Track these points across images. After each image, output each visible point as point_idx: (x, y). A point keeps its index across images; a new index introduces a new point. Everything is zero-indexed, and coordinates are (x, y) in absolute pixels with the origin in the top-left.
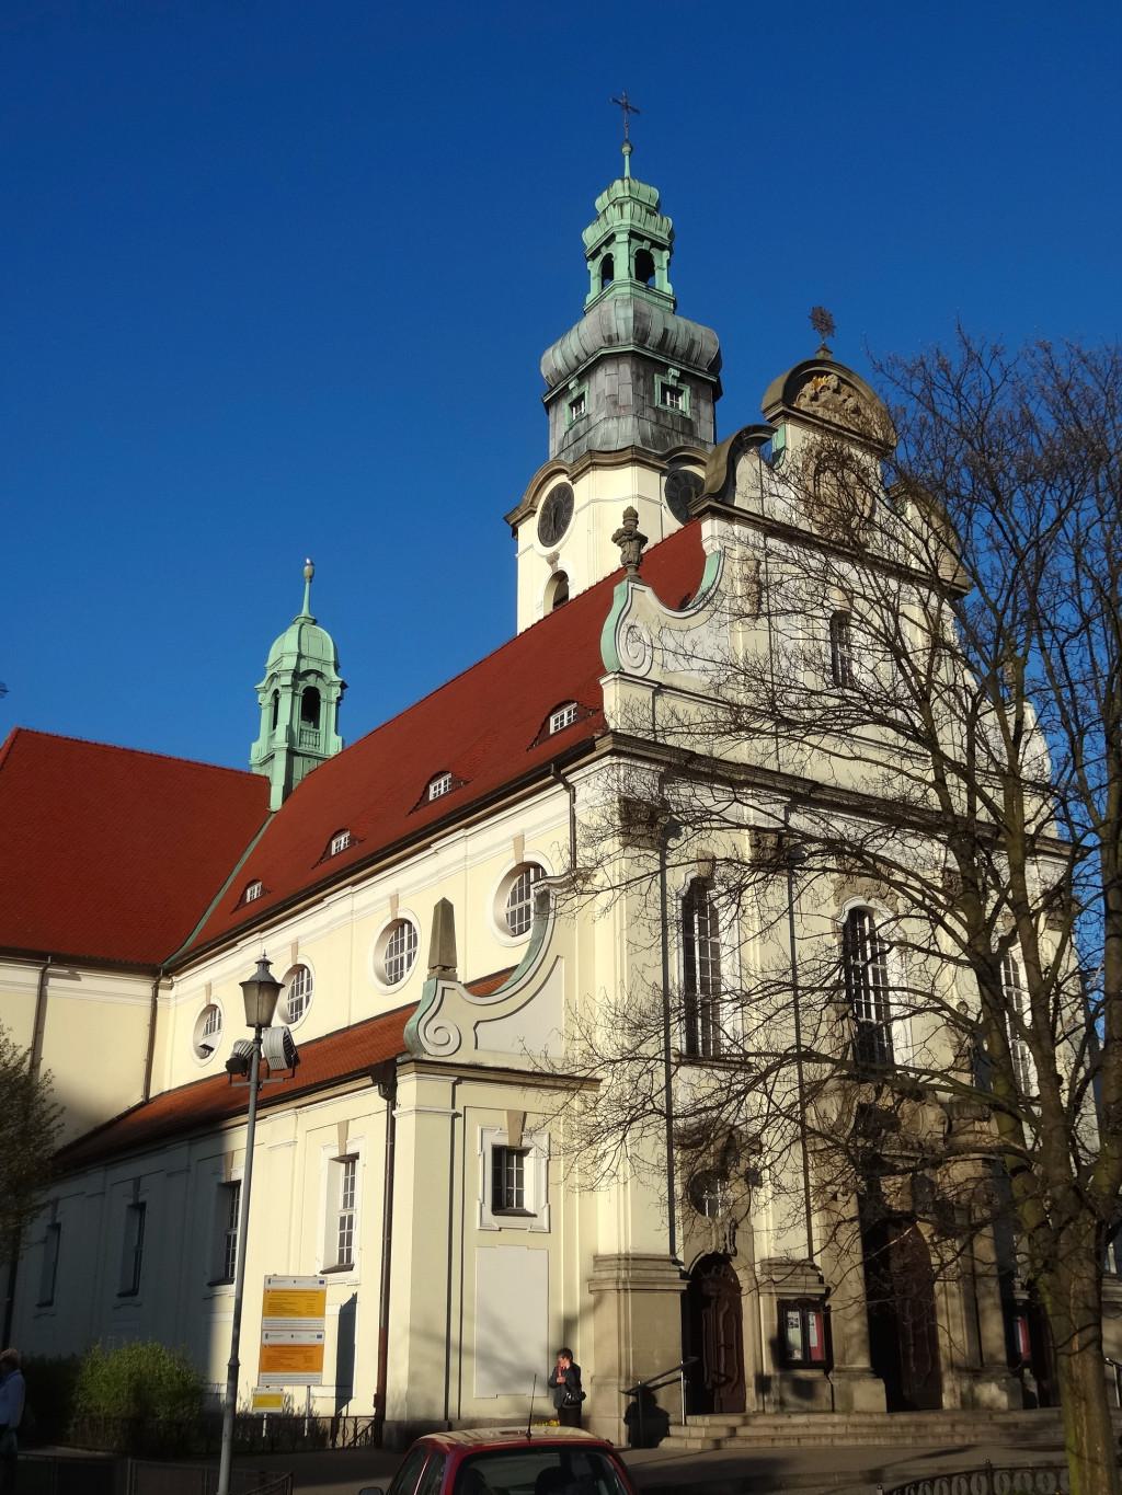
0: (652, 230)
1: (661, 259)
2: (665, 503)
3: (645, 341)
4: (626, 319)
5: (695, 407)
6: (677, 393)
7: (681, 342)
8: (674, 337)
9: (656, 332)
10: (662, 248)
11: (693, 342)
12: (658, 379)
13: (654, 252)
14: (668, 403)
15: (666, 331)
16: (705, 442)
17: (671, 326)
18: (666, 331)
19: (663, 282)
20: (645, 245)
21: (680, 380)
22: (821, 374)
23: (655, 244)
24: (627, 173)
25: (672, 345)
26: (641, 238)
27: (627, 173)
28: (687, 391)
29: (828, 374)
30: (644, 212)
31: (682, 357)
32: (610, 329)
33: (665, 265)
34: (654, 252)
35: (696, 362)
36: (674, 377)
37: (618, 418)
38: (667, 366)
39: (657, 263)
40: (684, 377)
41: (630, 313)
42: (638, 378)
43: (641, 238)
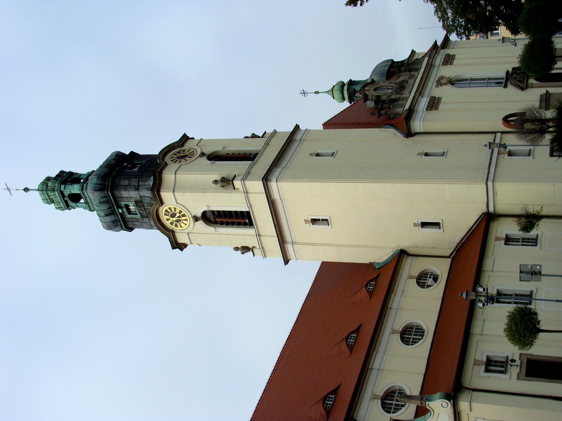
0: (59, 198)
3: (116, 220)
7: (105, 207)
9: (109, 219)
10: (62, 193)
11: (100, 203)
13: (67, 193)
15: (106, 215)
21: (121, 208)
23: (63, 196)
25: (108, 210)
31: (109, 203)
34: (67, 193)
35: (106, 197)
36: (122, 210)
38: (120, 214)
40: (119, 207)
43: (66, 202)
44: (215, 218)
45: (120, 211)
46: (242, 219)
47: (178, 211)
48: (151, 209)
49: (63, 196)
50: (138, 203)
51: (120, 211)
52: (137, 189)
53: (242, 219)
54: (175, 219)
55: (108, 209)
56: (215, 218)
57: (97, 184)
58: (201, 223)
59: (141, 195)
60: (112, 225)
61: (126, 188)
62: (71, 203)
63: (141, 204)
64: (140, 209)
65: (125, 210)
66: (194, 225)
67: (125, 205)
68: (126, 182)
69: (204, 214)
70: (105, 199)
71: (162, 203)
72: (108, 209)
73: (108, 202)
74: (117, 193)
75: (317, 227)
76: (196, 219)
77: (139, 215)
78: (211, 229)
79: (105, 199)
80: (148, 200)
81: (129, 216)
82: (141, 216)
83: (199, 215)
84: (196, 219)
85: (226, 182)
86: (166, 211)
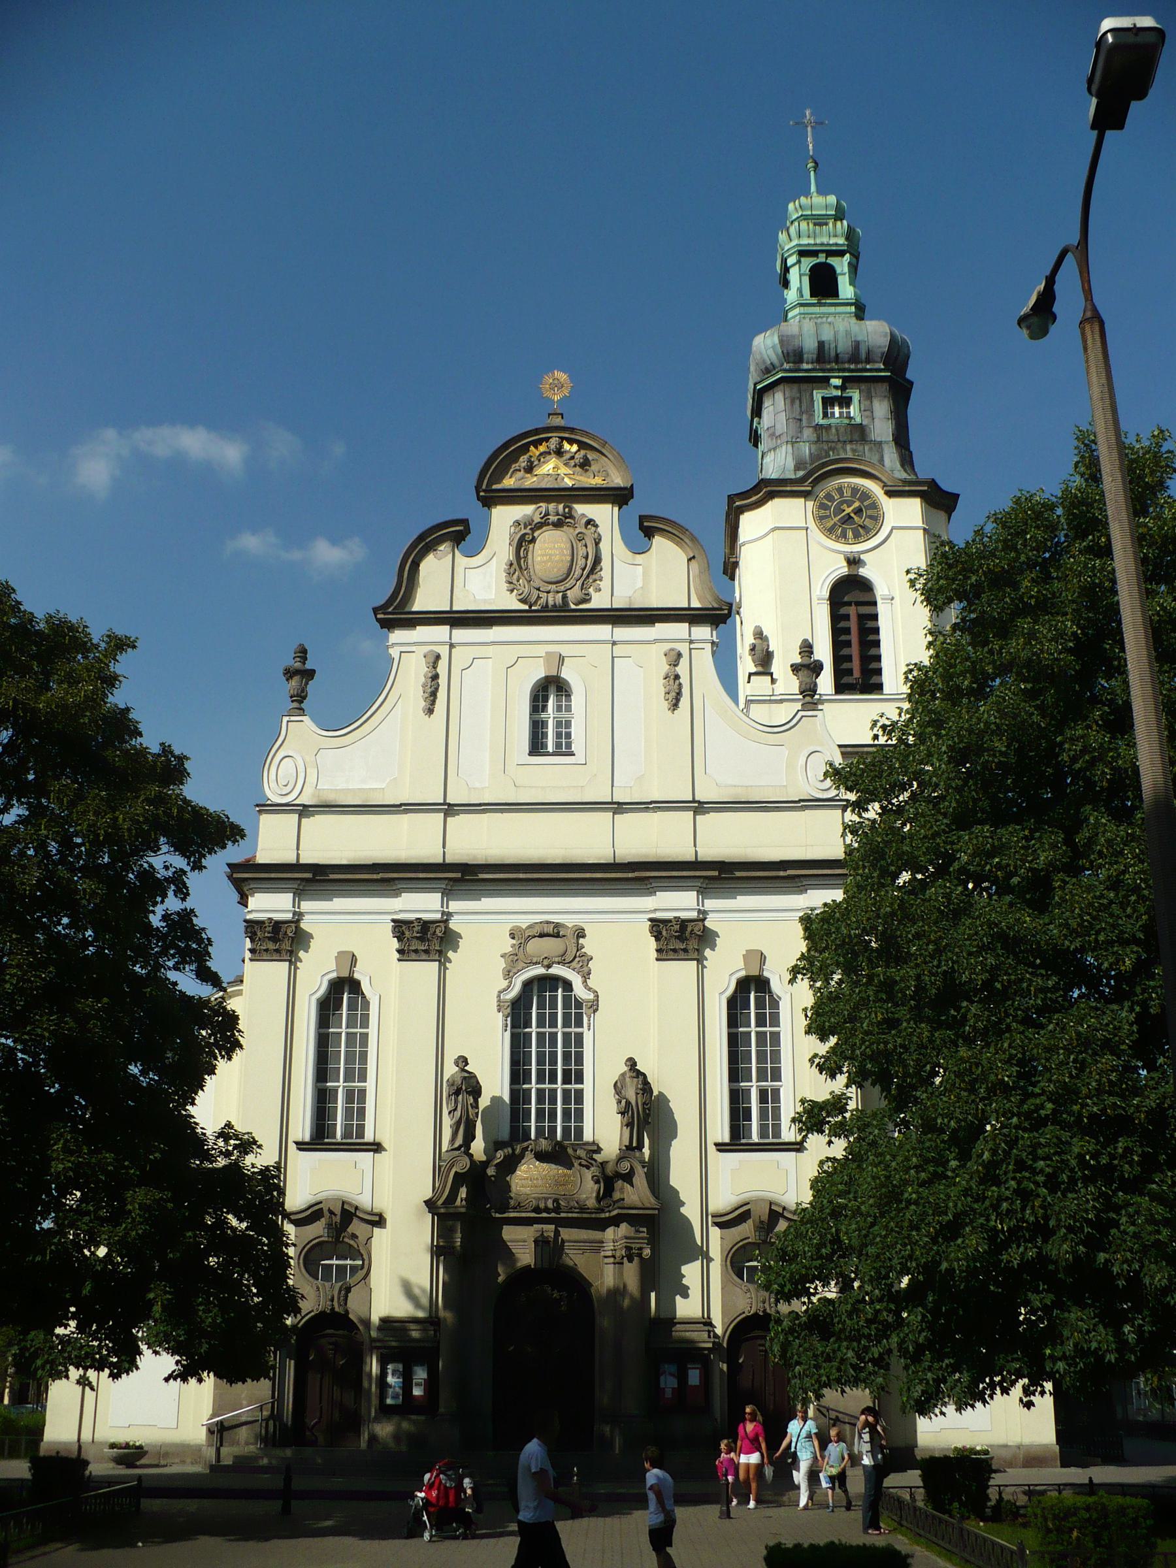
0: (825, 240)
1: (841, 265)
2: (812, 524)
4: (773, 347)
5: (868, 411)
6: (845, 402)
7: (844, 346)
8: (833, 346)
9: (810, 345)
10: (841, 254)
11: (857, 345)
12: (818, 395)
13: (832, 261)
14: (837, 415)
15: (821, 344)
16: (880, 443)
17: (827, 335)
18: (821, 344)
19: (846, 290)
20: (822, 258)
21: (843, 388)
22: (537, 444)
23: (830, 253)
24: (813, 188)
25: (833, 354)
26: (814, 253)
27: (813, 188)
28: (856, 395)
29: (547, 440)
30: (811, 226)
32: (764, 361)
33: (846, 269)
36: (836, 387)
37: (775, 449)
38: (827, 379)
39: (838, 271)
41: (776, 340)
42: (792, 401)
43: (814, 253)
45: (837, 382)
47: (868, 523)
49: (830, 253)
51: (837, 382)
55: (837, 355)
57: (899, 351)
58: (844, 570)
59: (885, 447)
60: (791, 348)
62: (808, 263)
63: (856, 437)
64: (842, 430)
65: (839, 393)
66: (839, 552)
67: (850, 398)
69: (865, 586)
70: (863, 356)
71: (890, 494)
72: (837, 355)
73: (855, 357)
74: (884, 387)
76: (854, 562)
77: (822, 422)
79: (863, 356)
81: (818, 395)
82: (818, 428)
83: (863, 572)
84: (854, 562)
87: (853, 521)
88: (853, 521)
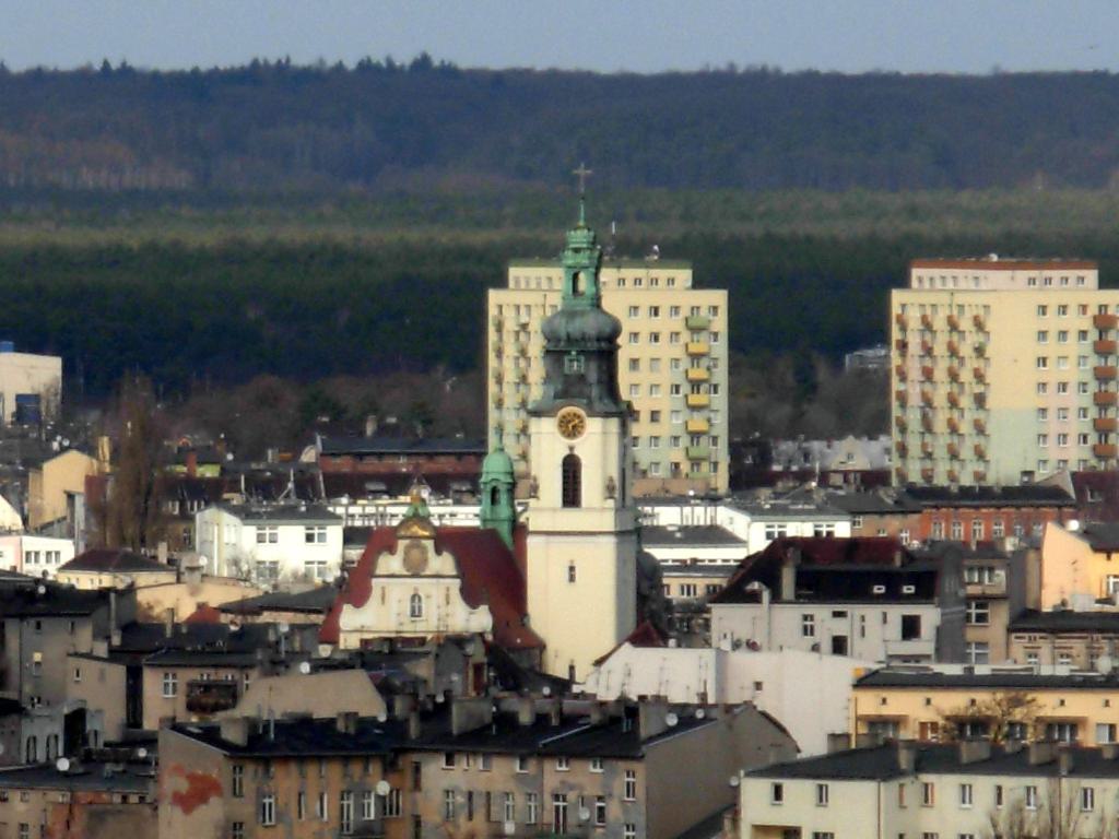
5: (587, 367)
9: (563, 334)
11: (584, 334)
17: (570, 330)
44: (571, 468)
45: (574, 353)
46: (571, 497)
48: (574, 390)
50: (582, 378)
52: (600, 382)
53: (571, 497)
54: (573, 423)
56: (571, 468)
58: (567, 452)
61: (599, 367)
68: (604, 368)
73: (583, 339)
75: (567, 570)
76: (571, 448)
78: (560, 462)
80: (586, 390)
83: (576, 452)
84: (571, 448)
85: (610, 489)
86: (579, 417)
87: (571, 429)
88: (571, 429)
